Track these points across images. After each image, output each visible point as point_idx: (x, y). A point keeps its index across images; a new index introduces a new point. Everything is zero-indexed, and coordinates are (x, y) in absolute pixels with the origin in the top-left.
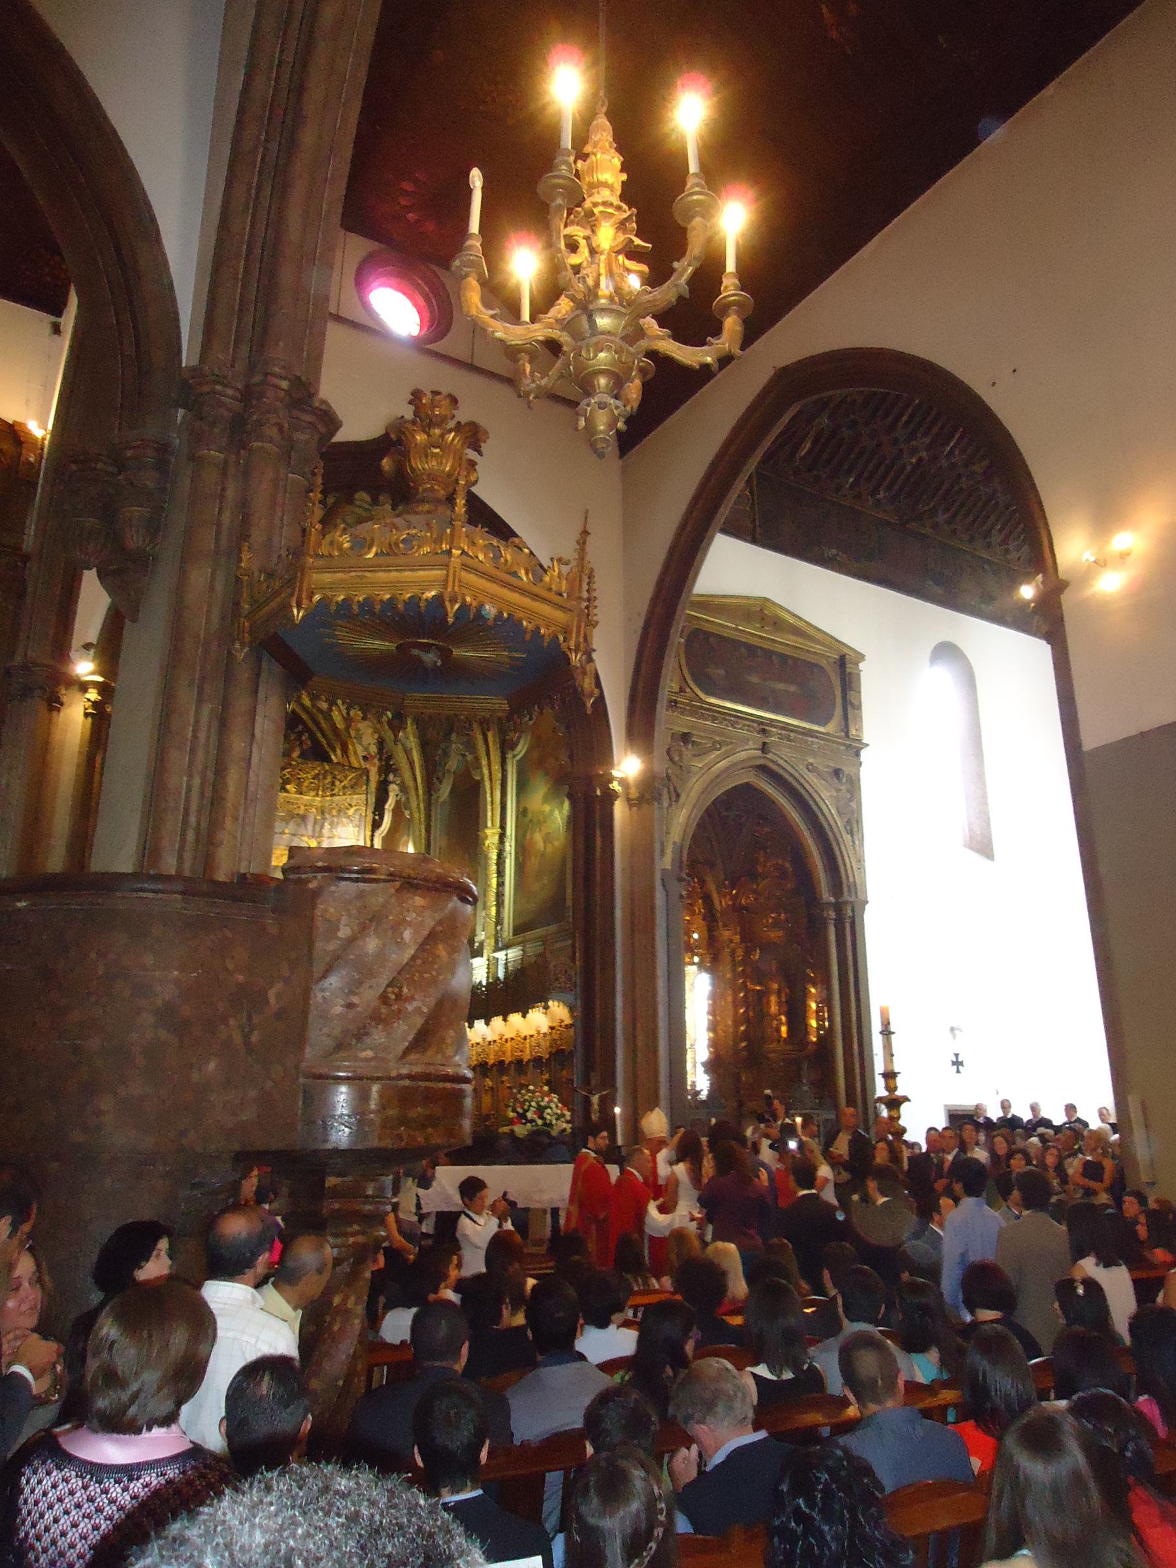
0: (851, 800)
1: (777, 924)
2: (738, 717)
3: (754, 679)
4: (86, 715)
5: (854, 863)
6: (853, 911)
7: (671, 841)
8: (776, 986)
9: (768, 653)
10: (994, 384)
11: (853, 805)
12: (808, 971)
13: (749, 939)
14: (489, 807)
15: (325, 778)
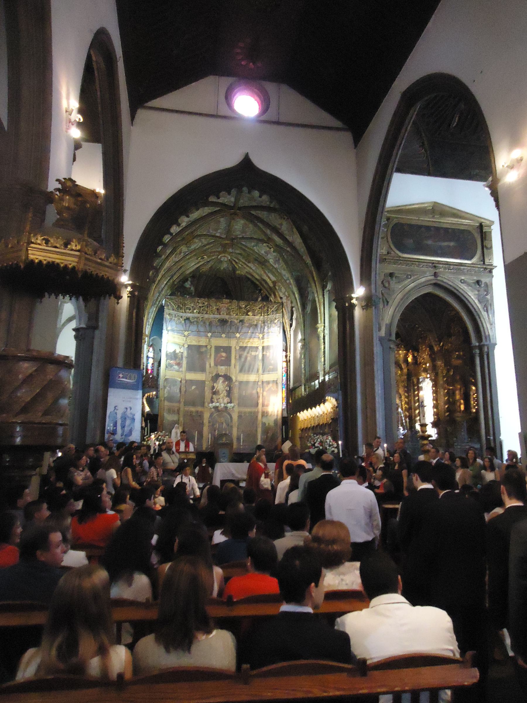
0: (486, 295)
1: (459, 357)
2: (420, 261)
3: (430, 242)
4: (128, 297)
5: (488, 326)
6: (488, 349)
7: (385, 323)
8: (459, 387)
9: (437, 229)
10: (474, 81)
11: (488, 297)
12: (471, 379)
13: (448, 364)
14: (319, 315)
15: (264, 307)
